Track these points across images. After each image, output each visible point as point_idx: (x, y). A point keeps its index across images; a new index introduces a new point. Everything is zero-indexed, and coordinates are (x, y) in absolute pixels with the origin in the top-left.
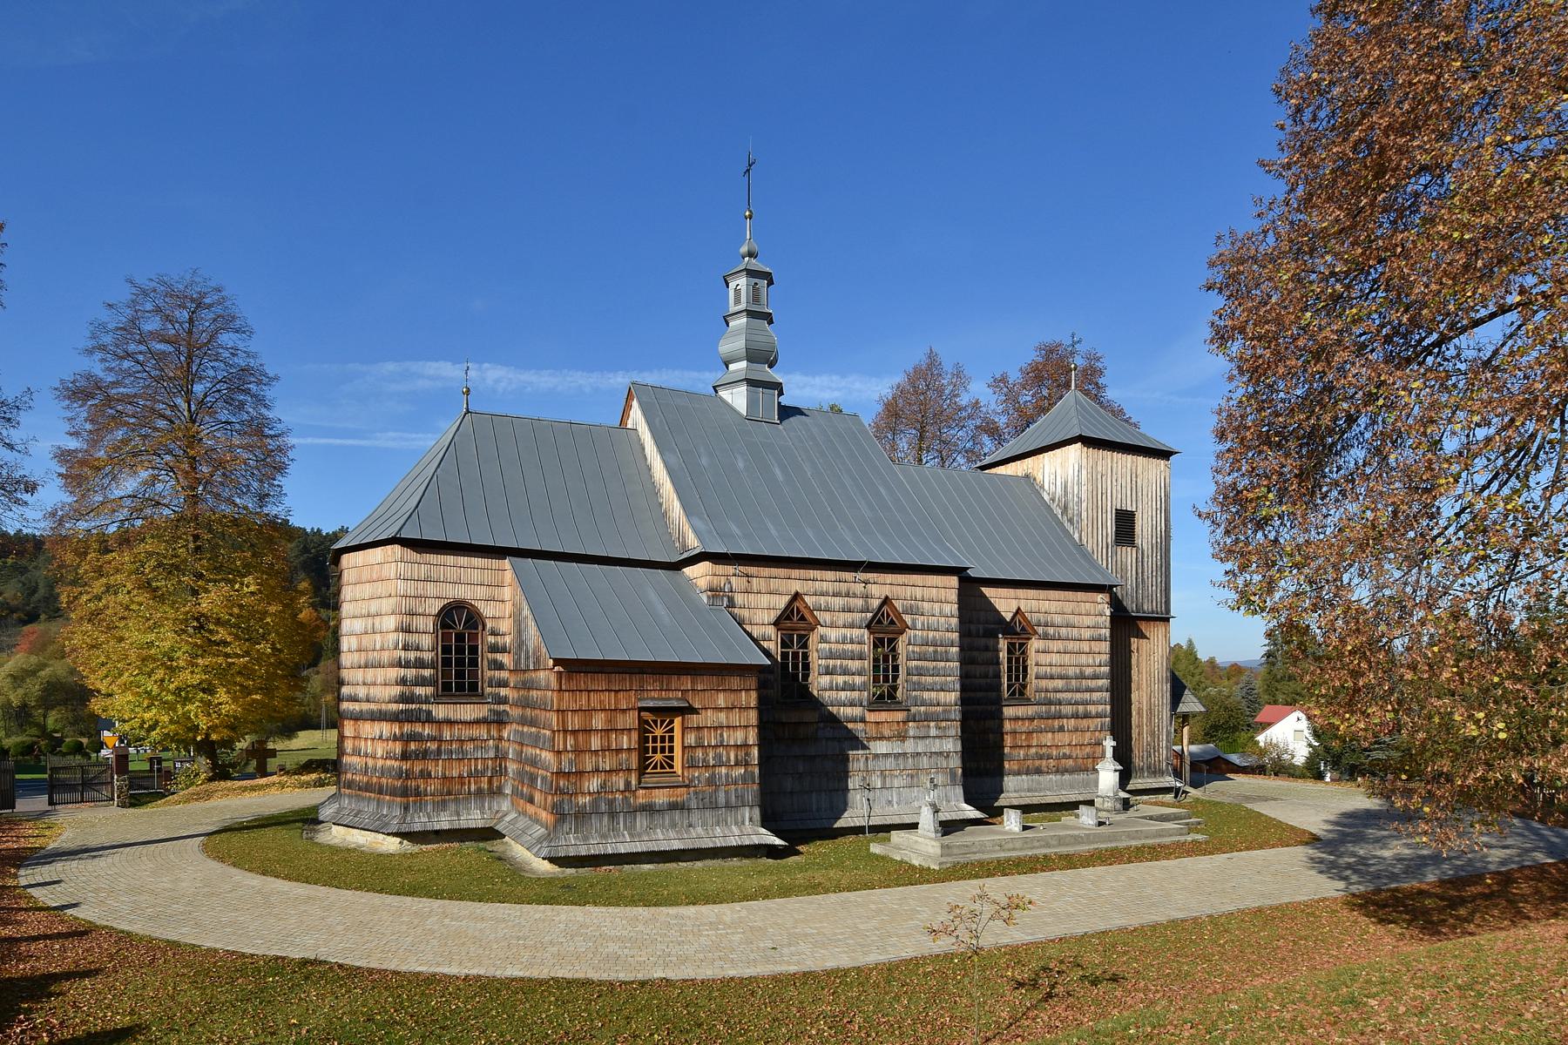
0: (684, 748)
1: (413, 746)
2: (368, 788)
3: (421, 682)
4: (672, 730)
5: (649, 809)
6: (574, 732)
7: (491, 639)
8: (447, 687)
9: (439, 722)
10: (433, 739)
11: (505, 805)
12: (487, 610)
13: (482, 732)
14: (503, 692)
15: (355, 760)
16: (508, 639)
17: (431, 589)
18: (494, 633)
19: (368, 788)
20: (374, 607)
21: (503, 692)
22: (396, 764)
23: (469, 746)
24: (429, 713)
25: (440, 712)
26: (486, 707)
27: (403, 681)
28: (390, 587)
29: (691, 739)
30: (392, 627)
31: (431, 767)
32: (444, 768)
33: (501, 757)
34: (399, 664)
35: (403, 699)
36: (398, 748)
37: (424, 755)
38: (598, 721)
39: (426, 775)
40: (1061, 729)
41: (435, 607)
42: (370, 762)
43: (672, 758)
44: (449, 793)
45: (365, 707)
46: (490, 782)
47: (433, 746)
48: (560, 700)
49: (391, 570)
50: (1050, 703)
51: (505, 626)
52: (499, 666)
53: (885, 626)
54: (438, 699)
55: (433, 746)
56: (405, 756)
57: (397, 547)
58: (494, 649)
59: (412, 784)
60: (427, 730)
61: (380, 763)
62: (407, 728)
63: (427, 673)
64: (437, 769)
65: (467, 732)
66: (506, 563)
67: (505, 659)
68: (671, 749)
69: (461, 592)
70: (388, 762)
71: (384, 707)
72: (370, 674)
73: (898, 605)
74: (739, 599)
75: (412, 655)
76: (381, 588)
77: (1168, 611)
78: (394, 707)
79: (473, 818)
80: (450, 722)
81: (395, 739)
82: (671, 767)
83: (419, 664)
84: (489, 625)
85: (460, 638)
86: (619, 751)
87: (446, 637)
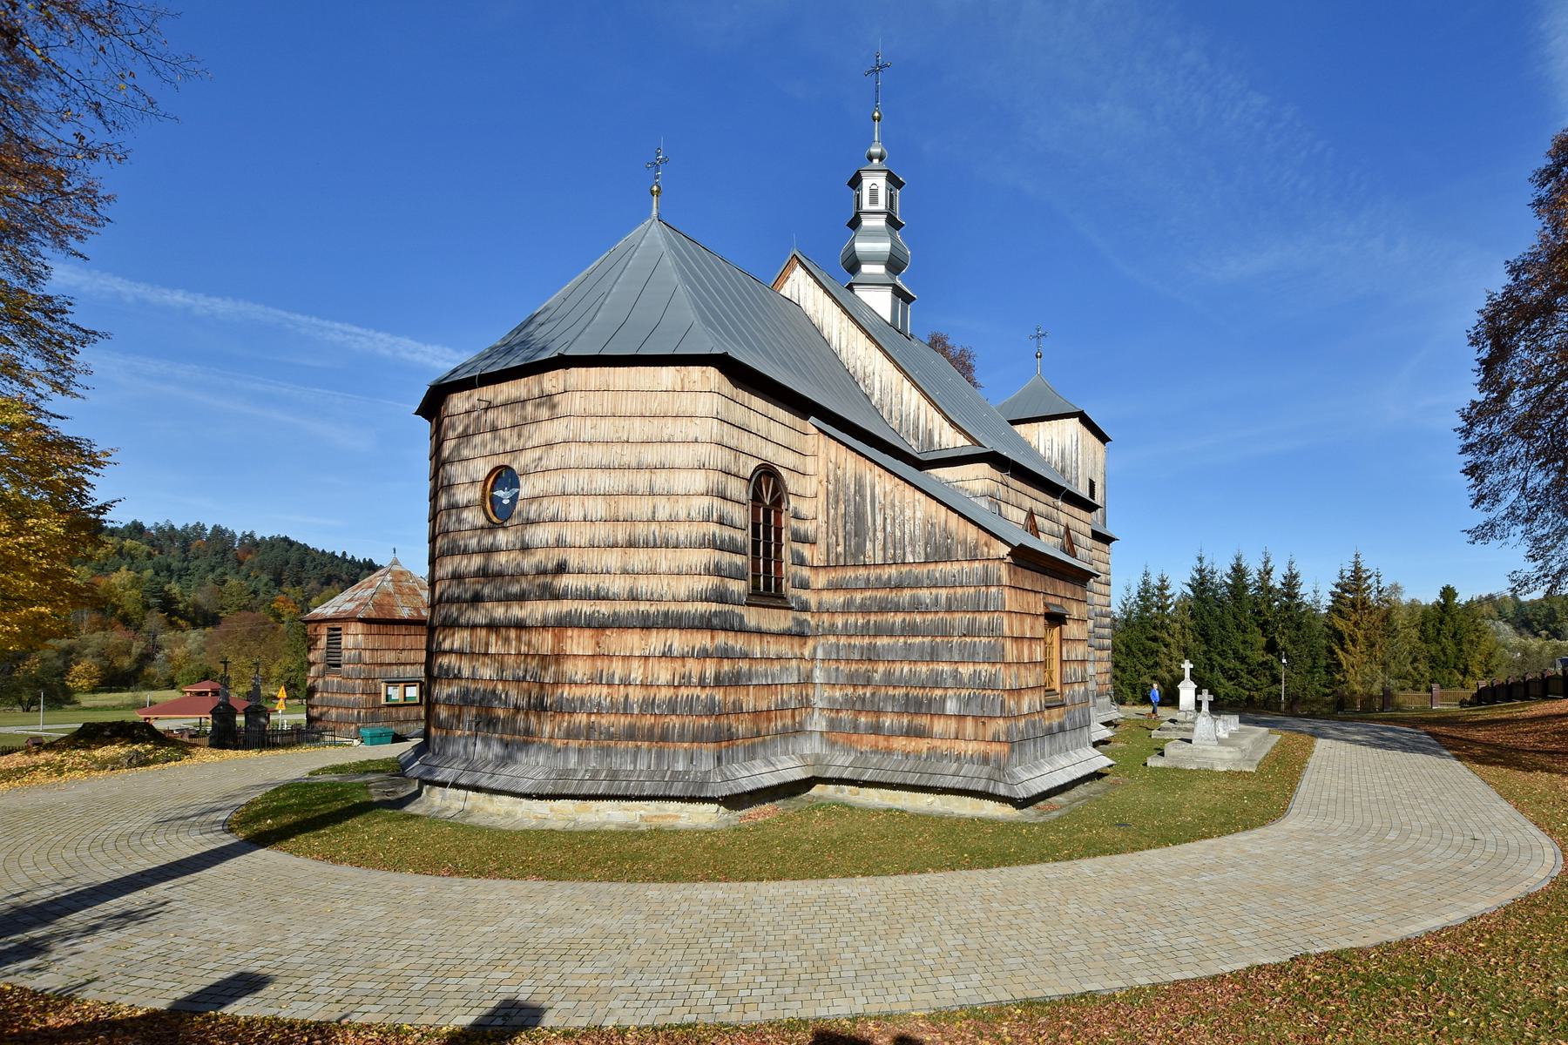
1: (726, 666)
2: (631, 734)
3: (738, 575)
5: (1050, 732)
11: (812, 746)
12: (791, 483)
13: (785, 647)
14: (805, 595)
15: (595, 692)
16: (808, 527)
17: (747, 443)
18: (796, 517)
19: (631, 734)
20: (651, 455)
21: (805, 595)
22: (703, 694)
23: (777, 667)
24: (741, 617)
25: (752, 617)
26: (791, 614)
27: (717, 571)
30: (702, 488)
33: (806, 681)
34: (703, 544)
35: (721, 597)
36: (710, 668)
39: (738, 710)
41: (749, 467)
42: (636, 694)
44: (758, 735)
45: (623, 608)
46: (793, 716)
49: (707, 404)
51: (806, 508)
56: (718, 682)
57: (712, 372)
59: (724, 721)
60: (737, 642)
61: (665, 694)
62: (721, 638)
63: (739, 560)
64: (750, 699)
65: (774, 647)
66: (811, 425)
67: (806, 550)
69: (770, 453)
70: (684, 692)
71: (673, 607)
72: (639, 558)
75: (727, 532)
78: (702, 607)
79: (790, 769)
80: (760, 632)
81: (704, 655)
83: (735, 549)
84: (793, 502)
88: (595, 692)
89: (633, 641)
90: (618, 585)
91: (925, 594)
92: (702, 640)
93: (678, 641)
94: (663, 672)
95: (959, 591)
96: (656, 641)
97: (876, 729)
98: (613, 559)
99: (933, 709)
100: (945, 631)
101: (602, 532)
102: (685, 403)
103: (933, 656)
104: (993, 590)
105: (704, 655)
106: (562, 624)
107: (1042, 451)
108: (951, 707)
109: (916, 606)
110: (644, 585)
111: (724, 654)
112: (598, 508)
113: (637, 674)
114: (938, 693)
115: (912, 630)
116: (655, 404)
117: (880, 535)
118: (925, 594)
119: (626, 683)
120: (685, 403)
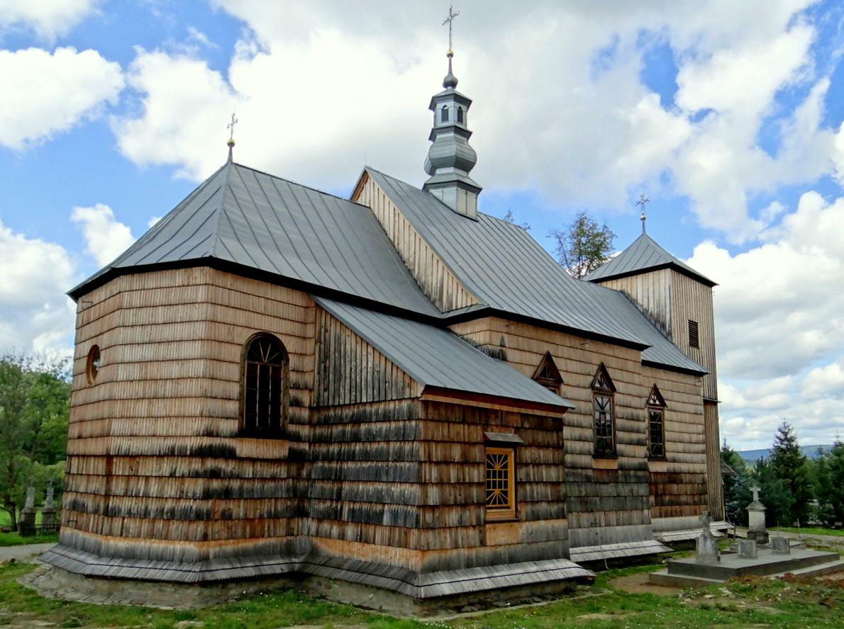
0: (517, 483)
4: (506, 466)
6: (437, 463)
7: (293, 377)
8: (250, 420)
9: (242, 460)
10: (232, 476)
13: (282, 471)
15: (126, 504)
17: (241, 318)
20: (167, 333)
25: (246, 448)
28: (199, 312)
29: (522, 473)
31: (232, 505)
32: (246, 510)
36: (199, 486)
37: (227, 494)
38: (456, 453)
40: (681, 482)
41: (244, 336)
43: (506, 493)
47: (235, 484)
48: (426, 428)
50: (674, 461)
52: (297, 403)
53: (604, 384)
54: (241, 434)
55: (235, 484)
56: (207, 495)
58: (296, 387)
60: (228, 466)
61: (169, 505)
62: (210, 464)
67: (306, 398)
68: (506, 486)
70: (183, 504)
72: (159, 408)
73: (610, 372)
74: (510, 354)
76: (182, 313)
77: (716, 399)
80: (253, 460)
81: (196, 475)
82: (506, 502)
85: (264, 369)
86: (471, 484)
87: (252, 369)
88: (126, 504)
89: (149, 467)
90: (144, 427)
91: (375, 427)
92: (196, 465)
93: (183, 467)
94: (171, 489)
95: (393, 425)
96: (166, 467)
97: (342, 537)
98: (142, 408)
99: (376, 519)
100: (381, 456)
101: (139, 389)
102: (189, 294)
103: (376, 477)
104: (413, 423)
105: (196, 475)
106: (109, 458)
107: (640, 301)
108: (386, 519)
109: (371, 438)
110: (162, 427)
111: (215, 474)
112: (136, 372)
113: (154, 488)
114: (379, 507)
115: (366, 456)
116: (174, 296)
117: (348, 381)
118: (375, 427)
119: (146, 496)
120: (189, 294)
